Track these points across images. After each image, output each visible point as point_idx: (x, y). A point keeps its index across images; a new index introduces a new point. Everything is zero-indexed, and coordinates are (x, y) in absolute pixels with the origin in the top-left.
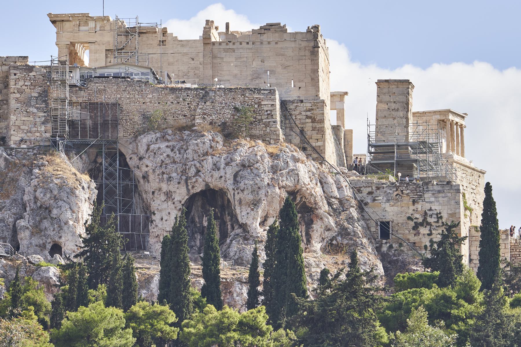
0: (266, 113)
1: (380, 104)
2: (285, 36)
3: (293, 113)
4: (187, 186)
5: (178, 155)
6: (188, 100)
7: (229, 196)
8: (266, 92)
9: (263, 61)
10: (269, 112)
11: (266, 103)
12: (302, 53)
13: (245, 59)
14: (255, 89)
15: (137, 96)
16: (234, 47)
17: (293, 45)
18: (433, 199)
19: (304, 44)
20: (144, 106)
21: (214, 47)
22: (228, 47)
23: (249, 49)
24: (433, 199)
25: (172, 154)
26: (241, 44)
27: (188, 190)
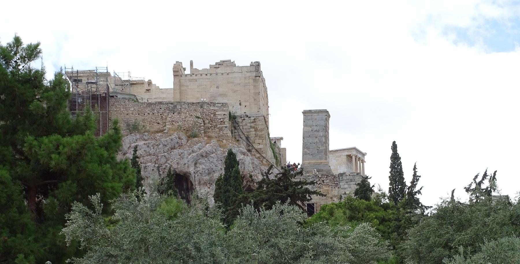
0: (220, 121)
1: (305, 128)
2: (235, 69)
3: (241, 124)
4: (159, 171)
5: (152, 150)
6: (161, 111)
7: (191, 179)
8: (220, 105)
9: (218, 87)
10: (222, 120)
11: (219, 113)
12: (247, 81)
13: (205, 86)
14: (211, 103)
15: (122, 109)
16: (196, 78)
17: (240, 75)
18: (346, 186)
19: (248, 74)
20: (128, 117)
21: (182, 78)
22: (192, 78)
23: (208, 79)
24: (346, 186)
25: (147, 149)
26: (201, 75)
27: (160, 175)
